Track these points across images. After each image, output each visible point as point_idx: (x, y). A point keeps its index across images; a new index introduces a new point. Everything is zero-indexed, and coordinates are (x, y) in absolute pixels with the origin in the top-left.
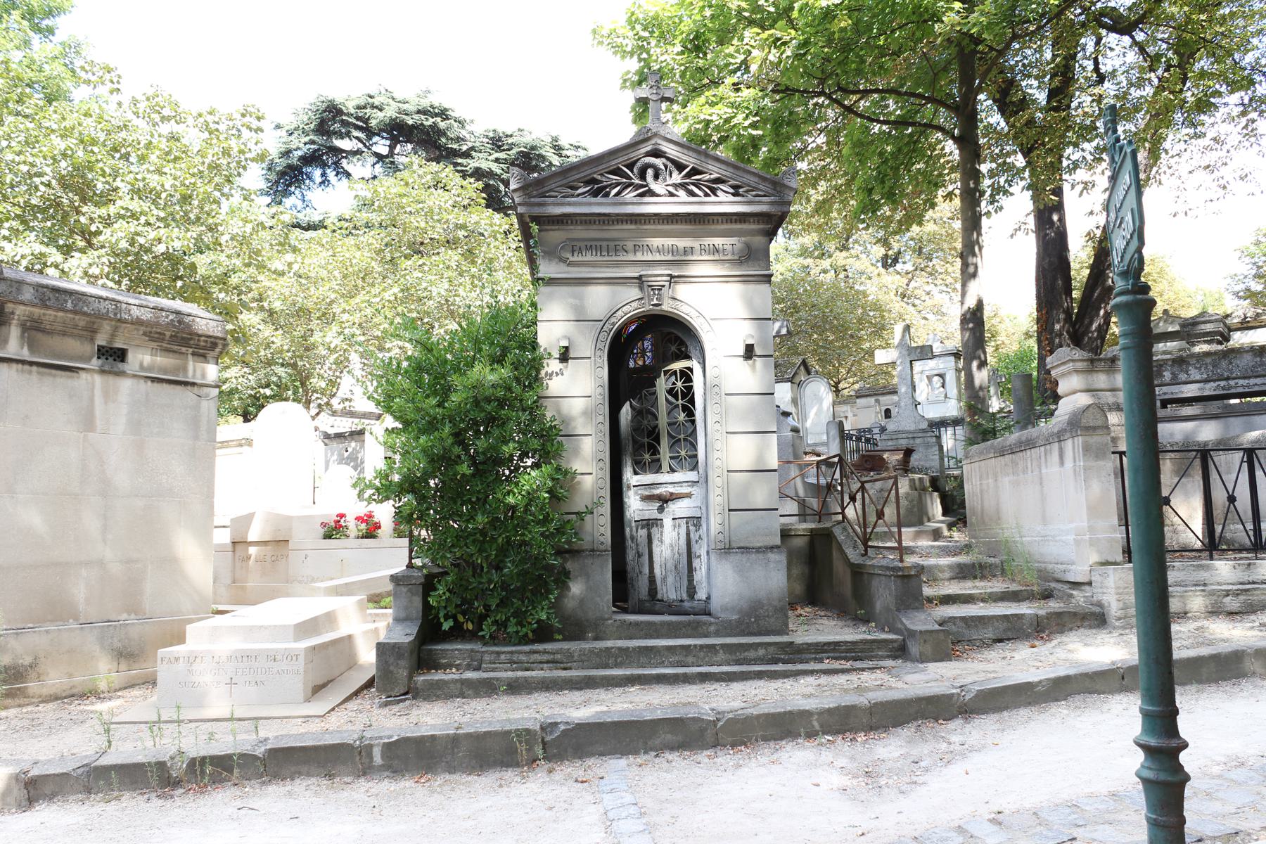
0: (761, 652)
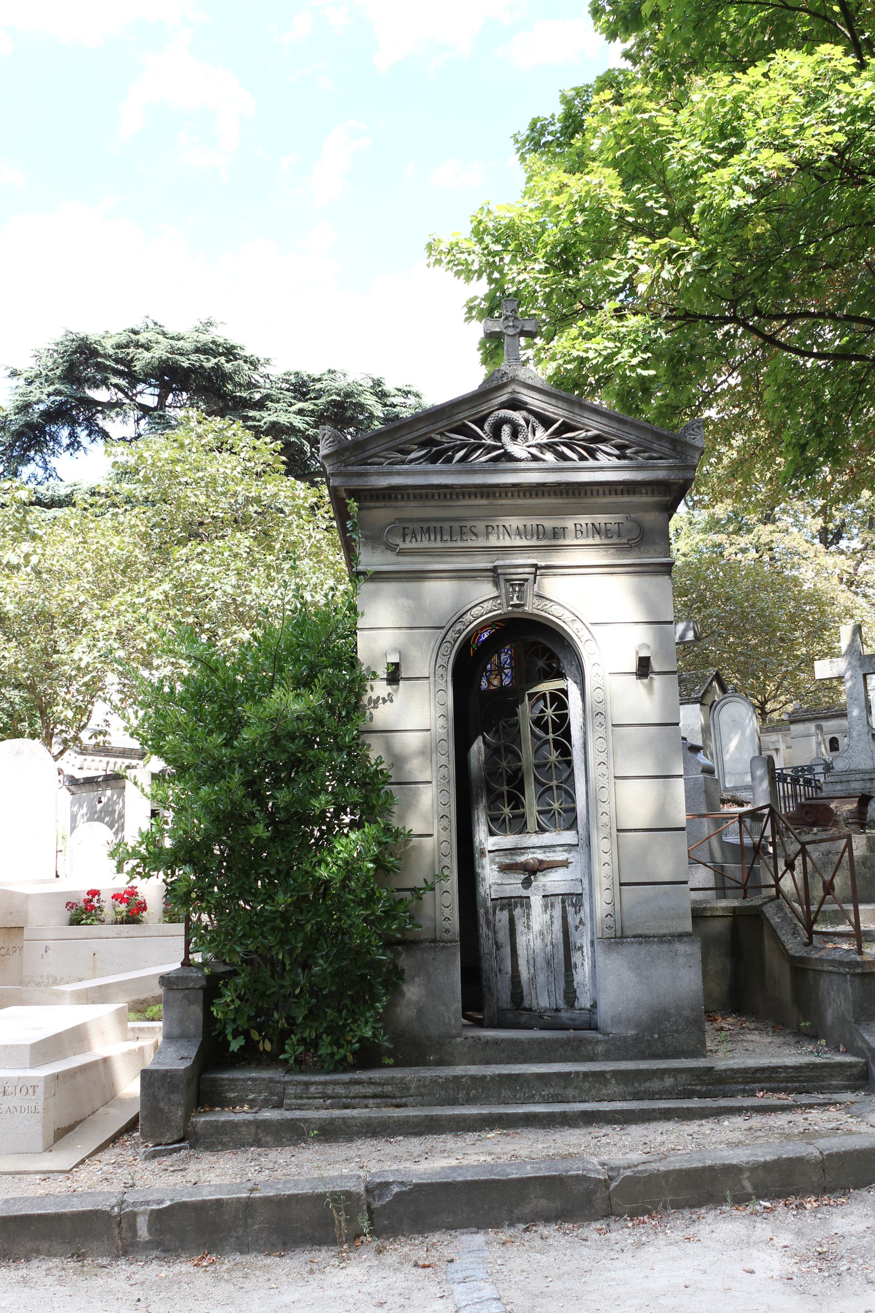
0: (669, 1082)
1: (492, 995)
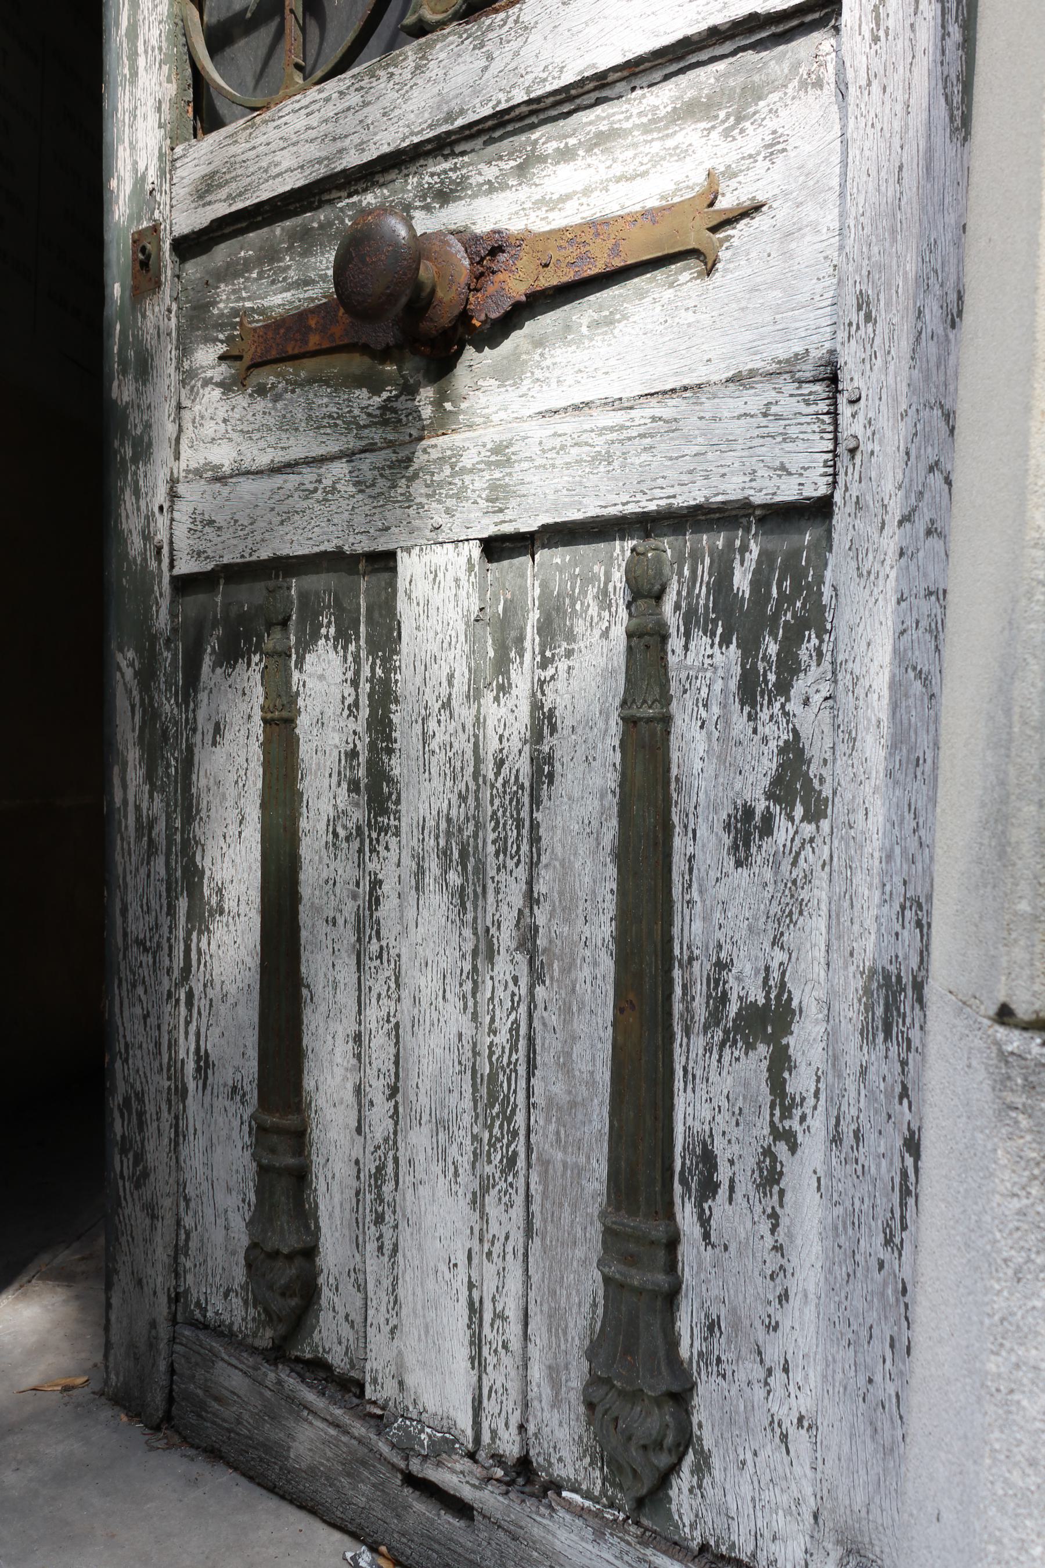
1: (152, 1211)
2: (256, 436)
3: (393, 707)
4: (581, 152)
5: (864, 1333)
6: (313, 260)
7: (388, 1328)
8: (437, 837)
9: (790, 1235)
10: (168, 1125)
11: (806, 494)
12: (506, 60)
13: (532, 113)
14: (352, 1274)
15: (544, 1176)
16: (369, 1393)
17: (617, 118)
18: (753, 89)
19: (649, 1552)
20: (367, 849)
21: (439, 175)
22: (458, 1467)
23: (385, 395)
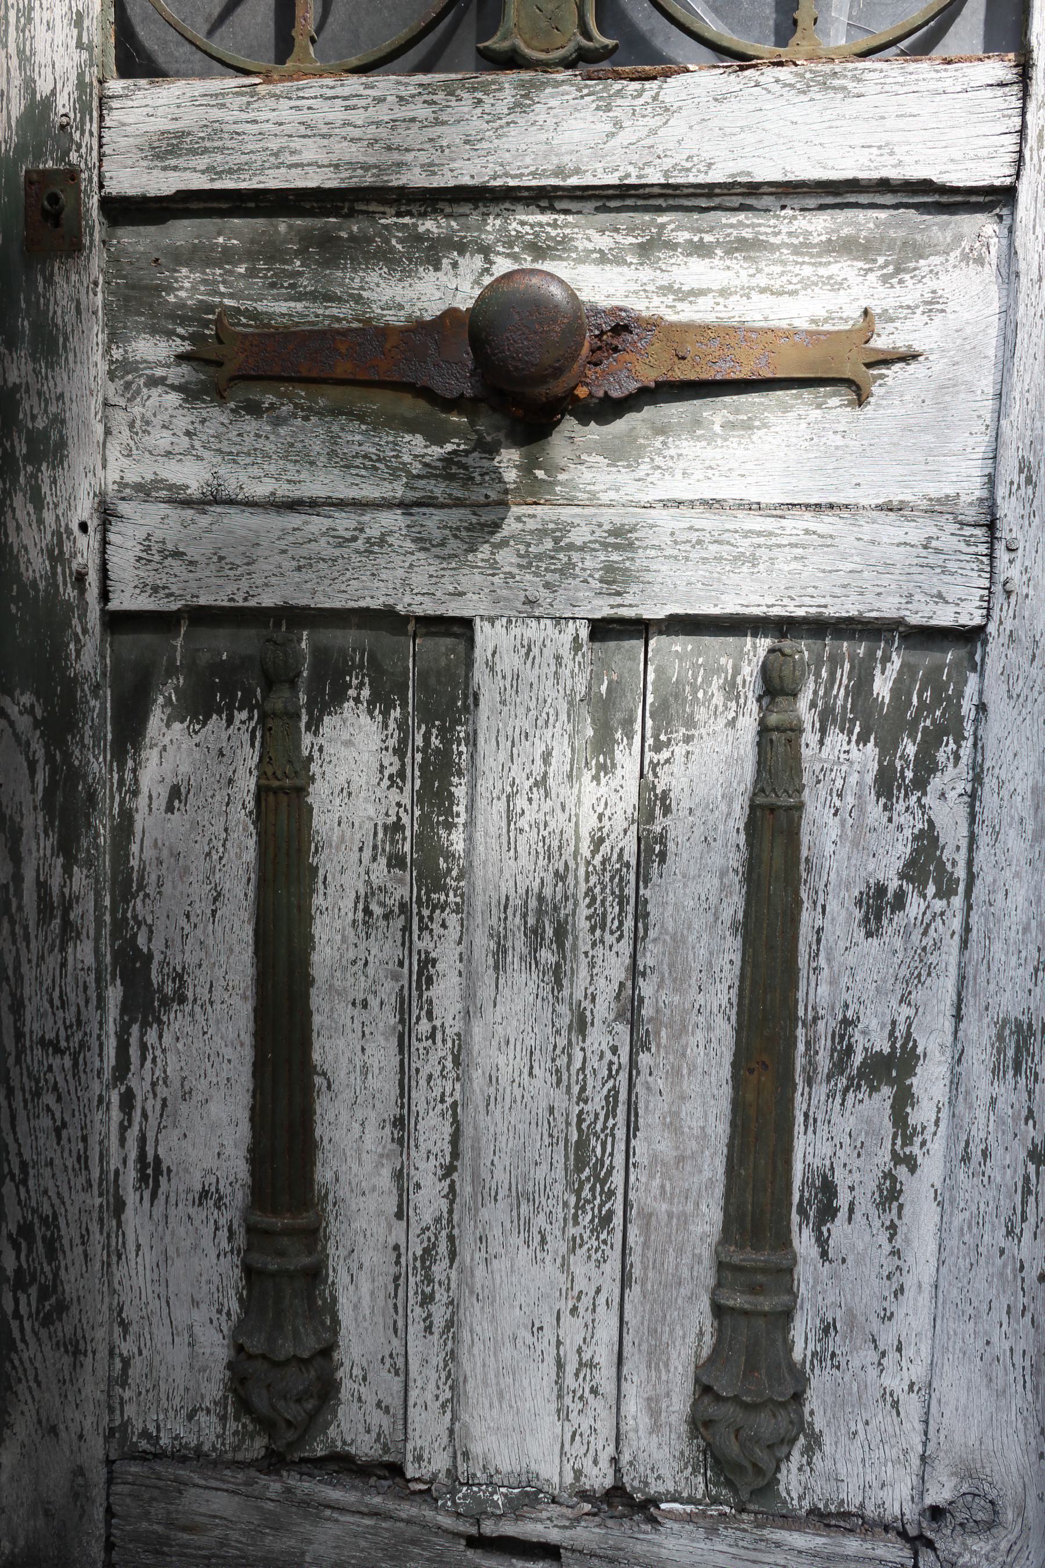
1: (75, 1349)
2: (243, 460)
3: (455, 780)
4: (719, 252)
5: (985, 1307)
6: (339, 274)
7: (438, 1404)
8: (525, 916)
9: (907, 1241)
10: (99, 1247)
11: (961, 622)
12: (638, 134)
13: (661, 196)
14: (388, 1361)
15: (646, 1229)
16: (411, 1472)
17: (763, 229)
18: (914, 246)
19: (765, 1532)
20: (415, 927)
21: (532, 226)
22: (545, 1515)
23: (449, 447)
